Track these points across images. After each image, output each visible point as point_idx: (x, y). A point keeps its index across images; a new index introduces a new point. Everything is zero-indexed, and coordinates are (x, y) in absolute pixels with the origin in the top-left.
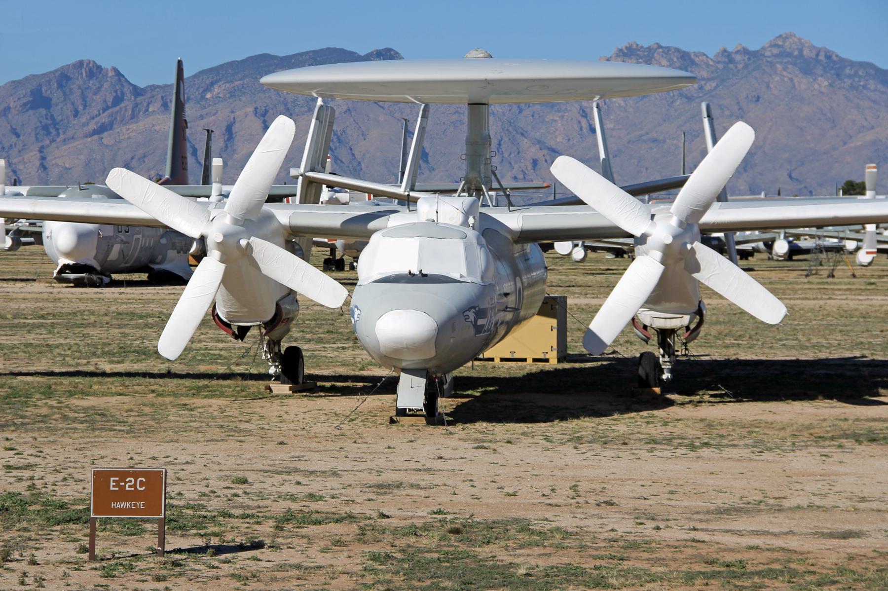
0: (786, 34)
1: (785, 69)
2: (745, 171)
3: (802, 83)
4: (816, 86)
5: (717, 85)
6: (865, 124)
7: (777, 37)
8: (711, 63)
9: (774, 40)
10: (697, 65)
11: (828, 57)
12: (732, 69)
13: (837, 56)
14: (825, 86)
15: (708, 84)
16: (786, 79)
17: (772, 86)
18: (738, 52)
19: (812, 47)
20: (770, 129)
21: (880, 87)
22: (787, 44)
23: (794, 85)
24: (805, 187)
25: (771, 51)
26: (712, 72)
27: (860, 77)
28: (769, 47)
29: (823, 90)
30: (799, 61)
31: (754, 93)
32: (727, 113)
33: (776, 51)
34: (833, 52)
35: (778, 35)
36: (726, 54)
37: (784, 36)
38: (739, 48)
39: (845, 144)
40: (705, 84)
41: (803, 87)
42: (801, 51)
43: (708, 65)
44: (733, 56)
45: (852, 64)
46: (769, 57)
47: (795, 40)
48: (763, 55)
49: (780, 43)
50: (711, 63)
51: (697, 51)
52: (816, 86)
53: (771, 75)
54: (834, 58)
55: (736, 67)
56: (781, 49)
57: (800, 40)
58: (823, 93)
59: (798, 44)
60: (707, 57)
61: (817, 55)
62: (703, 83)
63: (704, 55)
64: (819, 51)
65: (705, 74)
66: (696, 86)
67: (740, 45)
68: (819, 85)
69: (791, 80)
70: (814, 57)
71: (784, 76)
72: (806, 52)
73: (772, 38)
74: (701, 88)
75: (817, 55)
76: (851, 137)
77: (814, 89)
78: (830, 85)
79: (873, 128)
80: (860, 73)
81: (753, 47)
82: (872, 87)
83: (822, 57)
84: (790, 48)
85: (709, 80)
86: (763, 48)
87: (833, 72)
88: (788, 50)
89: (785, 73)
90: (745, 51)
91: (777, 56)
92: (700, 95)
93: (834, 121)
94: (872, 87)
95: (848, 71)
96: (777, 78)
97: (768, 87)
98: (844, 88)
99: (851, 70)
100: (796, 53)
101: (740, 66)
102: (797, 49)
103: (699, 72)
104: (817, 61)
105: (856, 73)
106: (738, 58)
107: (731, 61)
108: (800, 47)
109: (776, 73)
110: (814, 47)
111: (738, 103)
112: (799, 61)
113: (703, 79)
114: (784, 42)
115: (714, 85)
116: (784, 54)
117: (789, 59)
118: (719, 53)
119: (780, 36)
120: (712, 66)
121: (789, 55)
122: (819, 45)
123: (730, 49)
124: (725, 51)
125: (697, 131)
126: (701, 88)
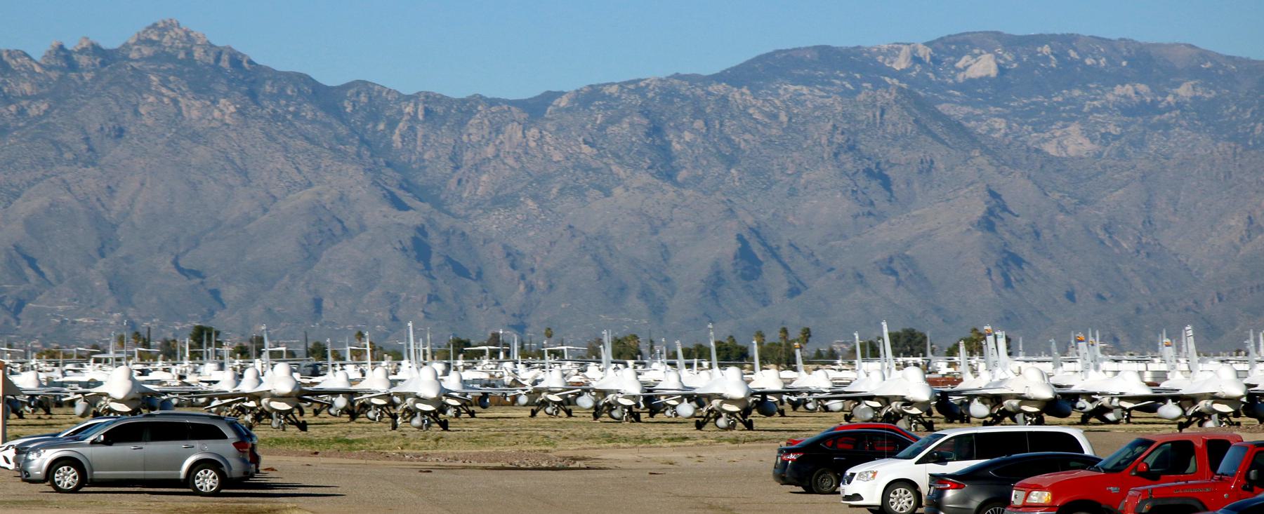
0: (164, 22)
1: (165, 83)
2: (102, 255)
3: (193, 109)
4: (217, 114)
5: (50, 106)
6: (298, 178)
7: (149, 28)
8: (38, 69)
9: (144, 32)
10: (13, 71)
11: (236, 60)
12: (73, 81)
13: (250, 62)
14: (232, 113)
15: (33, 106)
16: (166, 100)
17: (142, 110)
18: (83, 51)
19: (209, 46)
20: (142, 184)
21: (320, 114)
22: (166, 39)
23: (180, 110)
24: (202, 283)
25: (139, 50)
26: (41, 86)
27: (289, 98)
28: (135, 44)
29: (228, 120)
30: (186, 70)
31: (111, 124)
32: (68, 155)
33: (147, 51)
34: (244, 56)
35: (150, 24)
36: (62, 53)
37: (161, 25)
38: (85, 45)
39: (266, 210)
40: (29, 106)
41: (195, 114)
42: (189, 53)
43: (32, 73)
44: (75, 57)
45: (276, 76)
46: (137, 61)
47: (181, 33)
48: (126, 58)
49: (155, 38)
50: (38, 69)
51: (12, 48)
52: (217, 114)
53: (140, 94)
54: (245, 64)
55: (82, 78)
56: (155, 48)
57: (187, 33)
58: (228, 125)
59: (185, 39)
60: (31, 59)
61: (218, 59)
62: (24, 103)
63: (26, 55)
64: (221, 53)
65: (27, 88)
66: (13, 108)
67: (87, 38)
68: (221, 111)
69: (175, 101)
70: (212, 62)
71: (163, 95)
72: (198, 54)
73: (141, 29)
74: (22, 112)
75: (218, 59)
76: (275, 199)
77: (214, 119)
78: (240, 112)
79: (310, 185)
80: (289, 92)
81: (108, 44)
82: (309, 116)
83: (225, 63)
84: (171, 47)
85: (33, 98)
86: (126, 46)
87: (244, 88)
88: (171, 51)
89: (164, 90)
90: (96, 50)
91: (149, 59)
92: (21, 124)
93: (246, 174)
94: (309, 116)
95: (268, 88)
96: (151, 99)
97: (136, 113)
98: (262, 117)
99: (272, 86)
100: (182, 55)
101: (88, 77)
102: (183, 48)
103: (18, 85)
104: (220, 70)
105: (282, 93)
106: (84, 60)
107: (73, 66)
108: (188, 45)
109: (149, 90)
110: (212, 46)
111: (87, 139)
112: (186, 70)
113: (25, 97)
114: (161, 35)
115: (44, 107)
116: (162, 56)
117: (171, 66)
118: (50, 52)
119: (155, 26)
120: (39, 74)
121: (171, 58)
122: (219, 42)
123: (69, 47)
124: (61, 47)
125: (17, 187)
126: (22, 112)
